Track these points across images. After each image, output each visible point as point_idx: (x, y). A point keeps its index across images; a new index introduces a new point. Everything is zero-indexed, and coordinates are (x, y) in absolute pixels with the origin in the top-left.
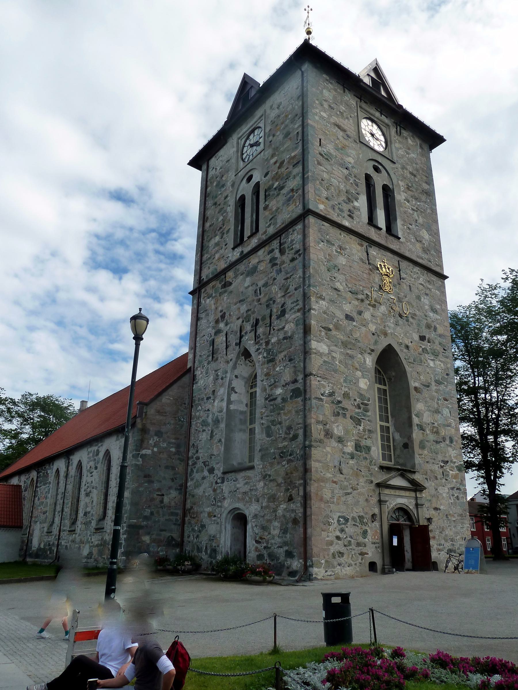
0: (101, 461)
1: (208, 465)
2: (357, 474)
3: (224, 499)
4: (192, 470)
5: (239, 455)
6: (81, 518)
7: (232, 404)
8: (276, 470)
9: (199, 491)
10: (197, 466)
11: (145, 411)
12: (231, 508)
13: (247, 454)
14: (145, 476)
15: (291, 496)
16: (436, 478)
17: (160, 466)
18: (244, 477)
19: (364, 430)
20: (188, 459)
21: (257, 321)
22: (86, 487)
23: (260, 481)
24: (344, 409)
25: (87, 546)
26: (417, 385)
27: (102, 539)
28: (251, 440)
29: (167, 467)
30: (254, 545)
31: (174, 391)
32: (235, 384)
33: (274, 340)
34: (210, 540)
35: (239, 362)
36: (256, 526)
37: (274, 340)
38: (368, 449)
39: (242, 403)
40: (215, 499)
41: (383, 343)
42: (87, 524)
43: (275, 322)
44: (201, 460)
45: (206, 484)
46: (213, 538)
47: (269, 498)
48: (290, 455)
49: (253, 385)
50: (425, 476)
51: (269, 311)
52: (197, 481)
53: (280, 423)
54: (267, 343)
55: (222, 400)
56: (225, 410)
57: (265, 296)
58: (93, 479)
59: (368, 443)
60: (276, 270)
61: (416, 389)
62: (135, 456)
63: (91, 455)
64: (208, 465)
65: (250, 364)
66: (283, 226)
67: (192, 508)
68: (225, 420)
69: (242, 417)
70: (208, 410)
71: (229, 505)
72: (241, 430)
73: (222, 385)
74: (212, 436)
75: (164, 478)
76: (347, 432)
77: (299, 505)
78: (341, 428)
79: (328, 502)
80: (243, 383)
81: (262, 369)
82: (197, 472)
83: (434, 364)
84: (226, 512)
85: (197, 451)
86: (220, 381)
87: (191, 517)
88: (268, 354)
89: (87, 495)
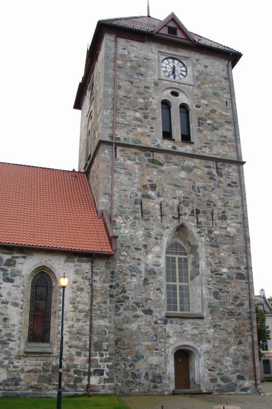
8: (225, 323)
15: (240, 341)
18: (193, 323)
23: (210, 328)
30: (206, 372)
36: (208, 359)
40: (156, 335)
47: (220, 341)
48: (238, 315)
53: (228, 292)
54: (210, 232)
71: (176, 342)
77: (248, 347)
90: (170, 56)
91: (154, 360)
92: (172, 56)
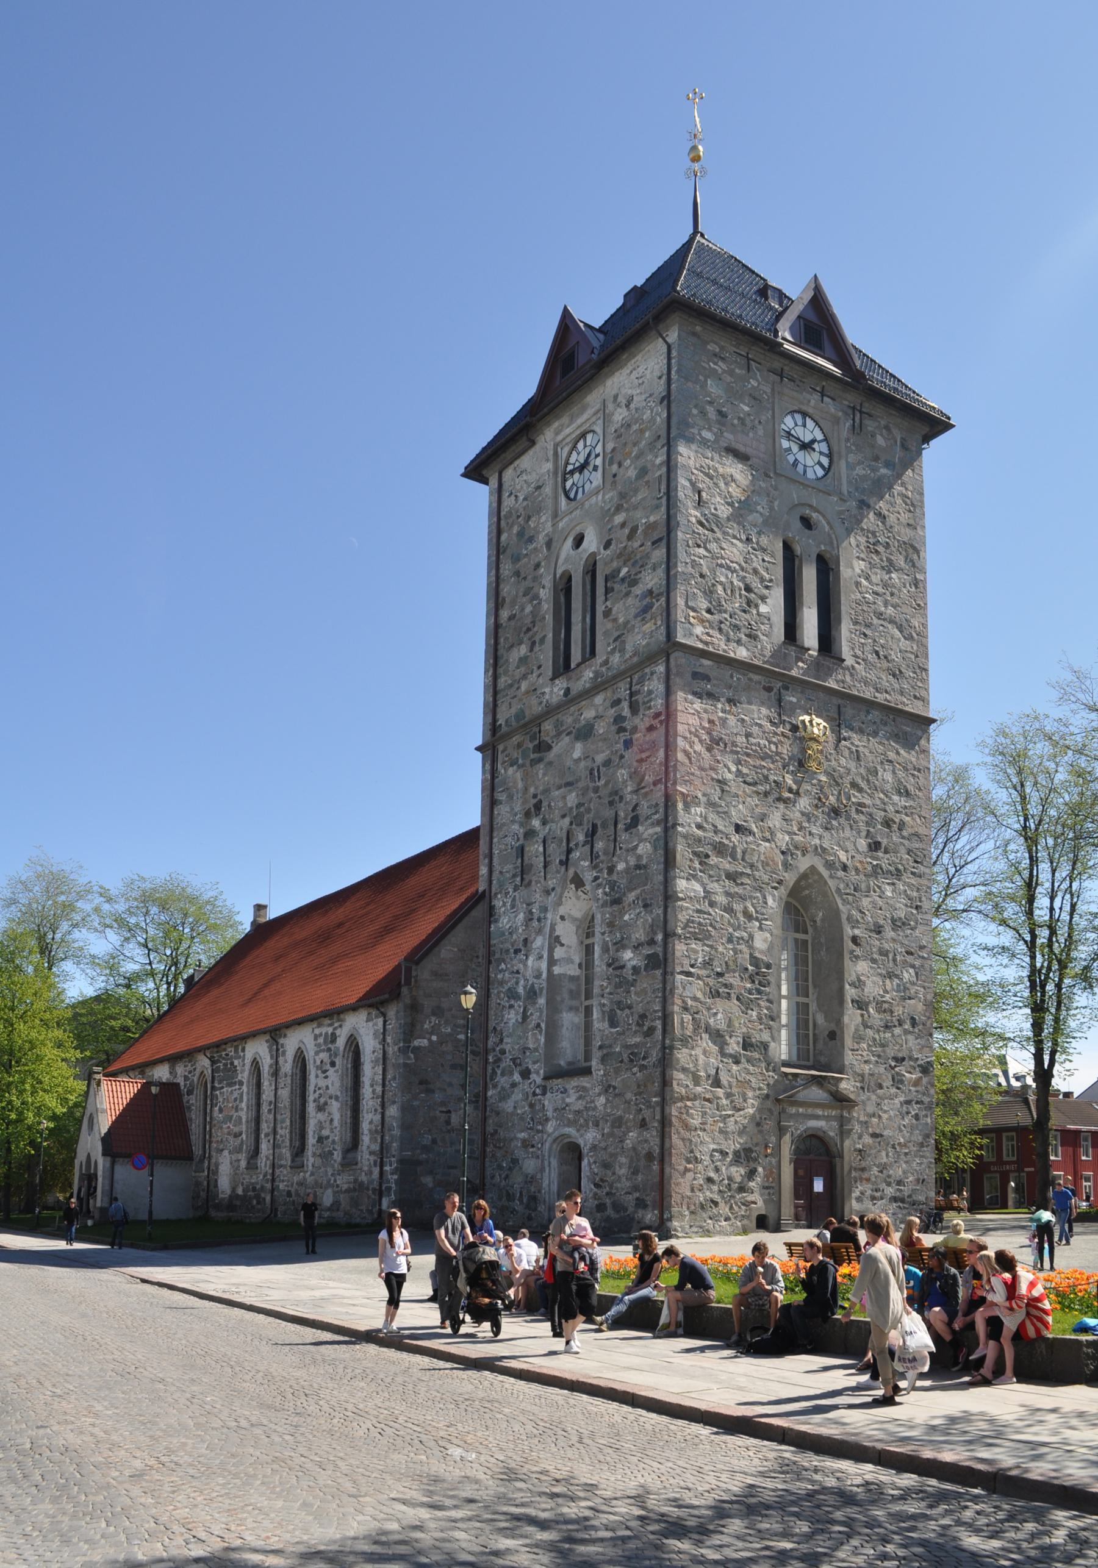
0: (341, 1053)
1: (520, 1065)
3: (547, 1120)
4: (493, 1069)
5: (569, 1048)
6: (313, 1145)
7: (555, 965)
9: (508, 1106)
10: (503, 1065)
11: (414, 974)
12: (556, 1134)
13: (582, 1047)
14: (421, 1083)
17: (442, 1065)
20: (487, 1052)
21: (594, 826)
22: (317, 1095)
25: (329, 1191)
27: (356, 1181)
28: (588, 1026)
29: (454, 1067)
31: (459, 936)
32: (559, 931)
33: (621, 866)
34: (526, 1182)
35: (566, 894)
37: (621, 866)
39: (572, 962)
40: (532, 1119)
42: (326, 1156)
43: (623, 836)
44: (509, 1056)
45: (517, 1096)
46: (530, 1180)
49: (589, 934)
51: (613, 812)
52: (503, 1088)
55: (541, 957)
56: (544, 975)
57: (607, 784)
58: (327, 1083)
60: (625, 741)
62: (404, 1051)
63: (321, 1040)
64: (520, 1065)
65: (584, 896)
66: (635, 659)
67: (496, 1131)
68: (545, 992)
69: (573, 987)
70: (518, 972)
71: (555, 1131)
72: (571, 1009)
73: (540, 931)
74: (525, 1017)
75: (450, 1085)
80: (574, 928)
81: (603, 914)
82: (503, 1074)
84: (550, 1140)
85: (501, 1040)
86: (535, 923)
87: (495, 1146)
88: (612, 889)
89: (321, 1108)
90: (574, 436)
91: (530, 1165)
92: (578, 432)
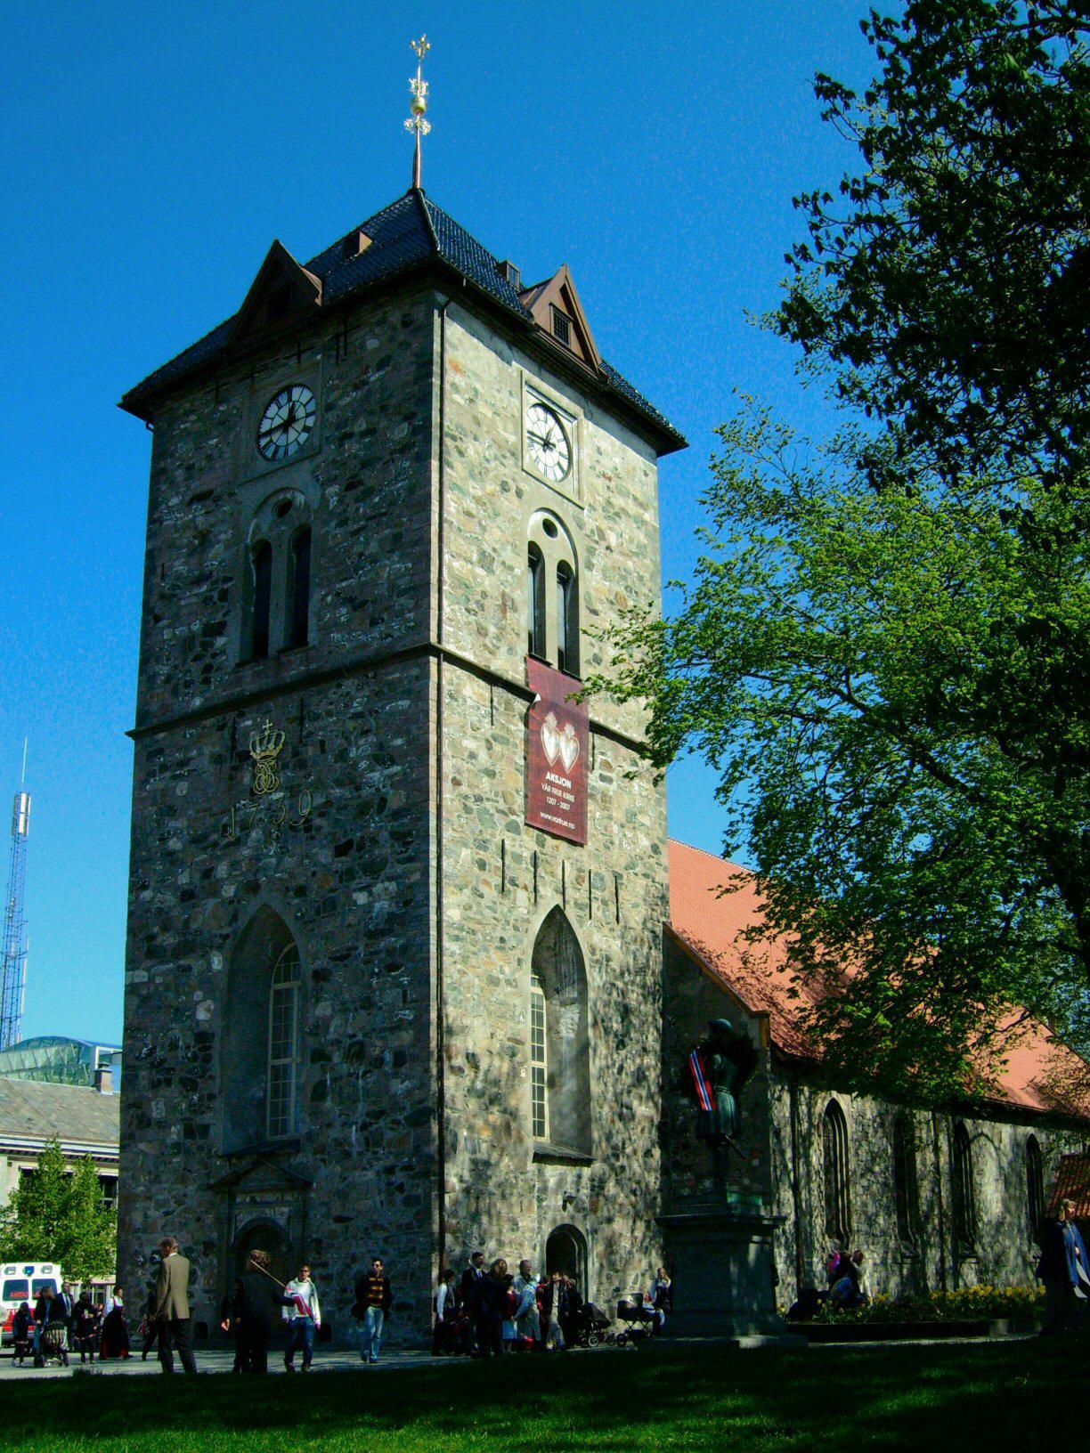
2: (183, 1180)
16: (347, 1155)
19: (200, 1099)
24: (169, 1070)
26: (318, 964)
38: (205, 1130)
41: (251, 906)
50: (319, 1156)
59: (207, 1118)
61: (320, 976)
76: (172, 1108)
78: (161, 1105)
79: (137, 1231)
83: (371, 894)
